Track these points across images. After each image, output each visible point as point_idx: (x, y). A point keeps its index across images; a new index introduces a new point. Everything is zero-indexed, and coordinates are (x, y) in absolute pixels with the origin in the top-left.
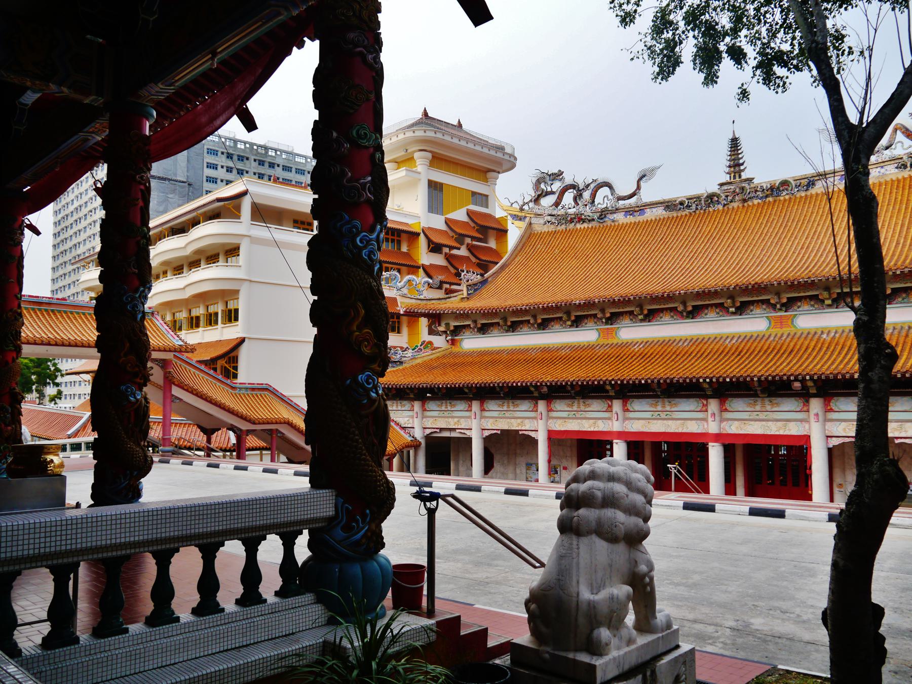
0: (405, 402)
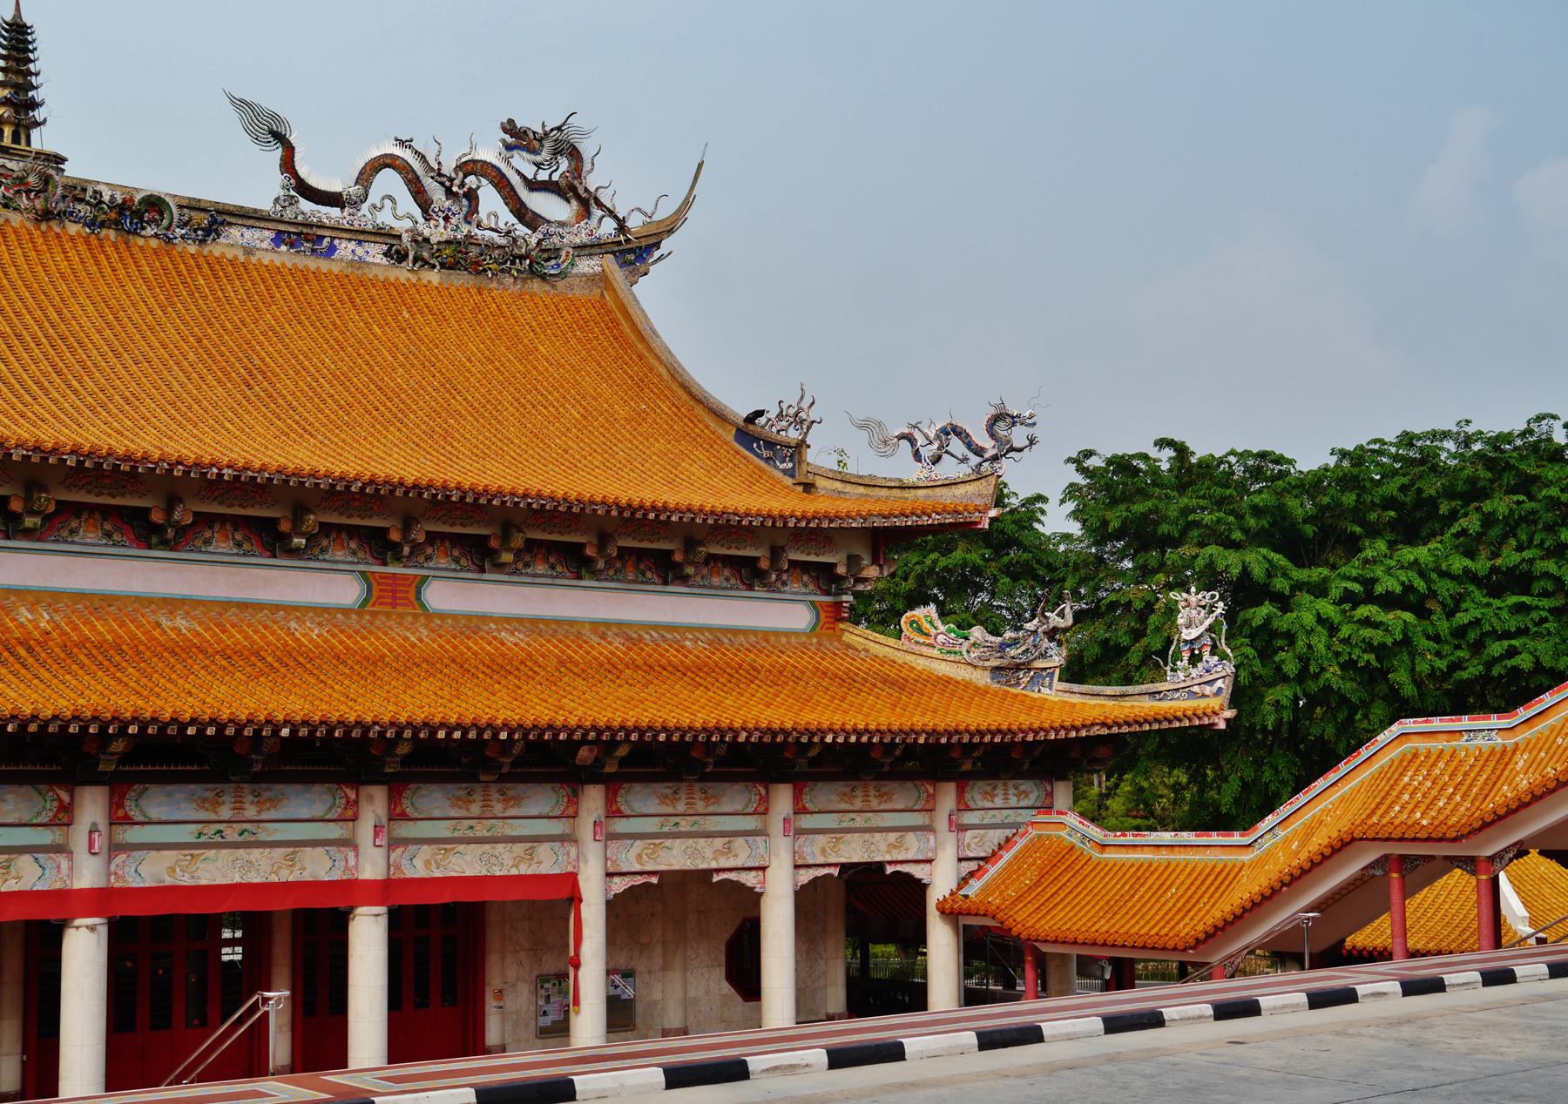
0: (1026, 785)
